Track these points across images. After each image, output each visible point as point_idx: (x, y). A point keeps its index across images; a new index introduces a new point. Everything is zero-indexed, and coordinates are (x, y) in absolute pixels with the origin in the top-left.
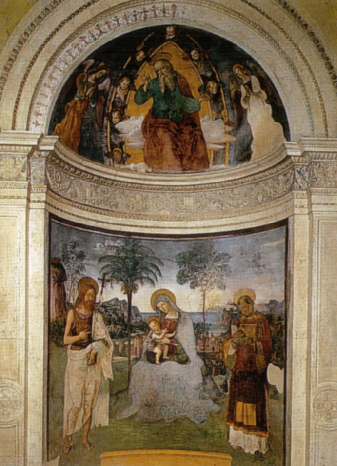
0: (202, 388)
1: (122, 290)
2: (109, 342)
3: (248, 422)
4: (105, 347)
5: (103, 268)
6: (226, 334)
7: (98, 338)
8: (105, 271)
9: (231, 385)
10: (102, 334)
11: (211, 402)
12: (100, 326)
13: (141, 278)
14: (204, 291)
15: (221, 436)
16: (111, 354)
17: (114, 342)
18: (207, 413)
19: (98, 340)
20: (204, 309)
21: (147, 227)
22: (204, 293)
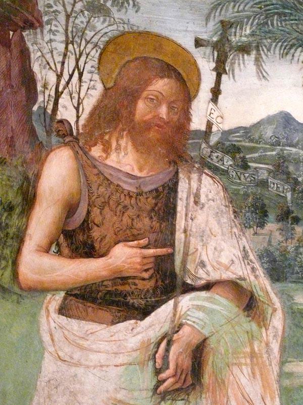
2: (259, 293)
4: (243, 318)
7: (203, 276)
10: (224, 260)
12: (216, 228)
16: (275, 347)
17: (286, 298)
19: (208, 287)
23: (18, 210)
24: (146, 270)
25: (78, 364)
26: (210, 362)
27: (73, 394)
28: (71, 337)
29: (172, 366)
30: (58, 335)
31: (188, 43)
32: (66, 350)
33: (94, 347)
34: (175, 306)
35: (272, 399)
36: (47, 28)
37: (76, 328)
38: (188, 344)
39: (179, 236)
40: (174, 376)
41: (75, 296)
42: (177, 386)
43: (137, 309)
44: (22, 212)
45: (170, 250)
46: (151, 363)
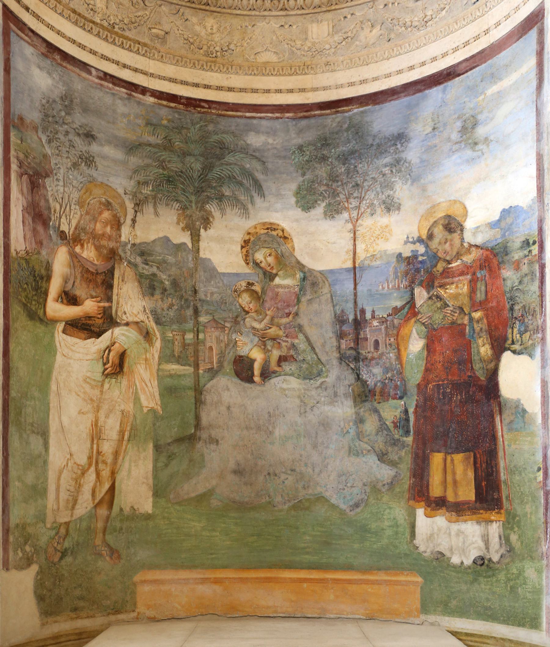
0: (352, 432)
1: (178, 223)
3: (456, 494)
5: (136, 171)
6: (403, 307)
8: (141, 178)
9: (417, 420)
11: (372, 460)
13: (220, 198)
14: (354, 222)
15: (397, 533)
18: (364, 485)
20: (354, 262)
21: (230, 89)
22: (354, 226)
23: (45, 279)
24: (100, 314)
25: (71, 358)
26: (127, 361)
27: (69, 372)
28: (68, 345)
29: (110, 361)
30: (62, 344)
31: (121, 191)
32: (66, 351)
33: (77, 350)
34: (112, 333)
35: (154, 381)
36: (55, 177)
37: (70, 340)
38: (118, 352)
39: (115, 298)
40: (111, 367)
41: (69, 324)
42: (113, 372)
43: (95, 333)
44: (47, 280)
45: (110, 304)
46: (101, 360)
